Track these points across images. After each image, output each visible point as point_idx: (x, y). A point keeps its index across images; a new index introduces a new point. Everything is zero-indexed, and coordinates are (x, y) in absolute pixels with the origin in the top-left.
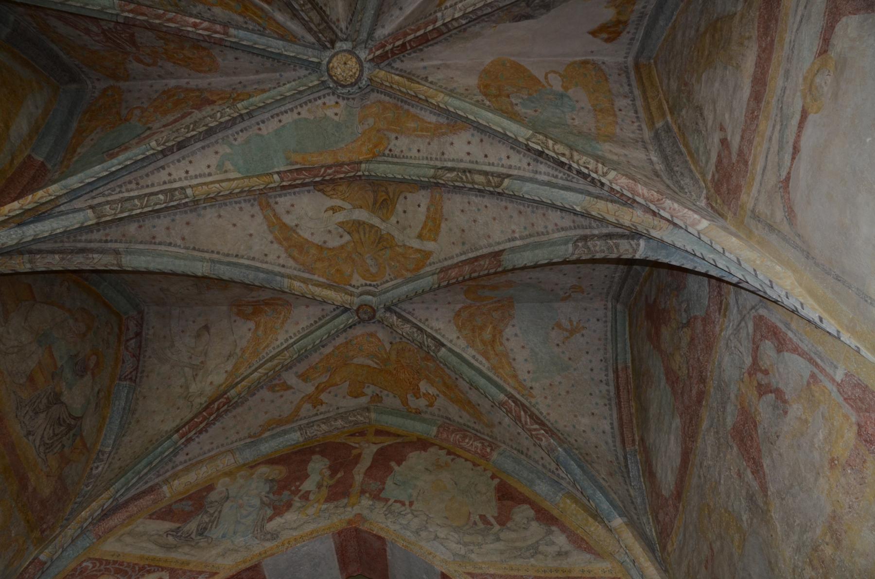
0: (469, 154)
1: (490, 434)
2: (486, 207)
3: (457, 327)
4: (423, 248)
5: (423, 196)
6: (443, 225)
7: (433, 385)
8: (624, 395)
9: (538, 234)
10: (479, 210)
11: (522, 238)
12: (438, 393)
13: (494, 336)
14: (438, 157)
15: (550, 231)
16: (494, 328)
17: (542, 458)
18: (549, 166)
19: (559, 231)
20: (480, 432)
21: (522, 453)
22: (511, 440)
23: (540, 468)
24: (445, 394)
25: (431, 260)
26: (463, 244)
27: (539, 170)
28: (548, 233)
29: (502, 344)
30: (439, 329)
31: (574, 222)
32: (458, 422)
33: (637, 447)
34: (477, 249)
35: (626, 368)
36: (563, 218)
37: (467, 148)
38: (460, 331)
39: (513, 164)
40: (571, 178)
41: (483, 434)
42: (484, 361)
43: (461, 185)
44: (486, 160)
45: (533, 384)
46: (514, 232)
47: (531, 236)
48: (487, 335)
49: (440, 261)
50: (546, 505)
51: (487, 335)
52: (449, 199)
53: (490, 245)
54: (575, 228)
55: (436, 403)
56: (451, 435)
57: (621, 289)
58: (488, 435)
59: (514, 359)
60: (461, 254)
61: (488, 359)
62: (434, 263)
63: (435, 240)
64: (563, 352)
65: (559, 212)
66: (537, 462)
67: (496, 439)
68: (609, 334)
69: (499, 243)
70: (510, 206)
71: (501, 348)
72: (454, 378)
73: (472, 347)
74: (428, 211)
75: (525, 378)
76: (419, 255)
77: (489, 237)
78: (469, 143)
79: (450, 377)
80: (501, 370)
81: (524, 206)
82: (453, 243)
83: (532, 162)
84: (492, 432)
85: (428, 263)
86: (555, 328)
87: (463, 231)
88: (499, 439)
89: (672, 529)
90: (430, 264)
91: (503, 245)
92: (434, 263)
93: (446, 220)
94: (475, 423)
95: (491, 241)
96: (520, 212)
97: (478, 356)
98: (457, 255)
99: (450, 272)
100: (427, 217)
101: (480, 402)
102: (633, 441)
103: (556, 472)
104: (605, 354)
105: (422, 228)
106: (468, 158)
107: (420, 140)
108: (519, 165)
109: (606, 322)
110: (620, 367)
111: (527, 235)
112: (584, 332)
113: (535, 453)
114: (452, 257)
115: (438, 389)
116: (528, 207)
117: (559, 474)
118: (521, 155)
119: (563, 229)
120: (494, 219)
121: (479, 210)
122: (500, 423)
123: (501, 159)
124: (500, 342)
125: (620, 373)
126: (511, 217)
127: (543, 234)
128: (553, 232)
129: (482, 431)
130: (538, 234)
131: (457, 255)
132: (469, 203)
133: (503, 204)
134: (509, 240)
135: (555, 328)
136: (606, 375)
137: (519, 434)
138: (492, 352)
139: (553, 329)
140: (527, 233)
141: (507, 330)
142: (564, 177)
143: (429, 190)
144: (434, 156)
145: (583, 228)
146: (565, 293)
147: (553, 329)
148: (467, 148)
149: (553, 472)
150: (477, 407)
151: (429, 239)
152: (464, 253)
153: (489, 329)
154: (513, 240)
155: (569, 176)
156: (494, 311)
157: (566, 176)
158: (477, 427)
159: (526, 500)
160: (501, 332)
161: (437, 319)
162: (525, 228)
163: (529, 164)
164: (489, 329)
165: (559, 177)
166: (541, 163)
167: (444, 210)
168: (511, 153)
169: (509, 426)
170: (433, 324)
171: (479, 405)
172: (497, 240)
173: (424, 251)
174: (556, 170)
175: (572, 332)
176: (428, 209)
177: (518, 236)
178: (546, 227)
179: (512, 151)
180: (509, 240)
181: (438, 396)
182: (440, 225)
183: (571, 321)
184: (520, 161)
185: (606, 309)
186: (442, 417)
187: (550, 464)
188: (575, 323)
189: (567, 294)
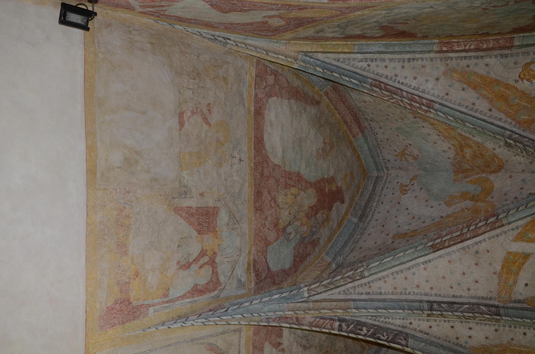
0: (470, 329)
1: (449, 62)
2: (451, 287)
3: (498, 157)
4: (524, 244)
5: (521, 294)
6: (499, 268)
7: (523, 93)
8: (349, 118)
9: (402, 271)
10: (459, 284)
11: (418, 265)
12: (516, 85)
13: (462, 151)
14: (502, 328)
15: (390, 275)
16: (464, 157)
17: (386, 67)
18: (392, 324)
19: (383, 277)
20: (461, 58)
21: (409, 60)
22: (423, 67)
23: (387, 56)
24: (508, 86)
25: (516, 232)
26: (477, 252)
27: (401, 321)
28: (392, 274)
29: (453, 145)
30: (515, 156)
31: (370, 287)
32: (491, 57)
33: (322, 93)
34: (463, 249)
35: (354, 137)
36: (380, 288)
37: (471, 333)
38: (494, 154)
39: (425, 322)
40: (373, 319)
41: (457, 58)
42: (463, 133)
43: (465, 314)
44: (452, 324)
45: (415, 120)
46: (425, 269)
47: (409, 269)
48: (468, 152)
49: (505, 232)
50: (363, 42)
51: (468, 152)
52: (491, 292)
53: (449, 254)
54: (369, 283)
55: (520, 70)
56: (494, 44)
57: (374, 190)
58: (451, 58)
59: (438, 135)
60: (480, 242)
61: (461, 135)
62: (513, 229)
63: (509, 253)
64: (404, 140)
65: (383, 292)
66: (391, 60)
67: (441, 59)
68: (379, 152)
69: (440, 257)
70: (428, 291)
71: (453, 142)
72: (493, 110)
73: (478, 143)
74: (516, 280)
75: (424, 123)
76: (530, 235)
77: (450, 262)
78: (470, 337)
79: (499, 109)
80: (446, 127)
81: (414, 292)
82: (488, 251)
83: (408, 325)
84: (447, 65)
85: (520, 229)
86: (416, 156)
87: (477, 264)
88: (439, 59)
89: (255, 84)
90: (517, 228)
91: (436, 256)
92: (513, 229)
93: (495, 273)
94: (468, 66)
95: (448, 258)
96: (418, 286)
97: (470, 136)
98: (485, 240)
99: (488, 229)
100: (518, 274)
101: (463, 93)
102: (327, 94)
103: (369, 62)
104: (376, 139)
105: (523, 264)
106: (471, 325)
107: (523, 344)
108: (420, 322)
109: (384, 159)
110: (360, 134)
111: (413, 268)
112: (396, 153)
113: (394, 68)
114: (490, 238)
115: (516, 89)
116: (410, 292)
117: (366, 62)
118: (418, 329)
119: (380, 279)
120: (444, 278)
121: (459, 284)
122: (437, 79)
123: (437, 325)
124: (456, 147)
125: (358, 130)
126: (427, 281)
127: (397, 272)
128: (388, 276)
129: (459, 61)
130: (402, 271)
131: (485, 240)
132: (469, 289)
133: (434, 292)
134: (430, 261)
135: (416, 156)
136: (370, 124)
137: (415, 78)
138: (459, 139)
139: (418, 156)
140: (412, 270)
141: (453, 155)
142: (379, 318)
143: (513, 299)
144: (507, 328)
145: (361, 285)
146: (413, 185)
147: (418, 156)
148: (471, 333)
149: (372, 60)
150: (465, 86)
151: (516, 254)
152: (476, 243)
153: (468, 156)
154: (426, 262)
155: (375, 320)
156: (469, 169)
157: (377, 320)
158: (465, 62)
159: (382, 37)
160: (457, 154)
161: (520, 163)
162: (414, 274)
163: (411, 323)
164: (468, 156)
165: (383, 318)
166: (399, 326)
167: (497, 281)
168: (428, 331)
169: (427, 81)
170: (522, 159)
171: (463, 89)
172: (441, 259)
173: (523, 241)
174: (386, 322)
175: (403, 153)
176: (515, 282)
177: (421, 265)
178: (394, 278)
179: (427, 332)
180: (430, 261)
181: (516, 81)
182: (502, 268)
183: (407, 161)
184: (419, 325)
185: (387, 168)
186: (512, 55)
187: (377, 66)
188: (404, 159)
189: (412, 183)
